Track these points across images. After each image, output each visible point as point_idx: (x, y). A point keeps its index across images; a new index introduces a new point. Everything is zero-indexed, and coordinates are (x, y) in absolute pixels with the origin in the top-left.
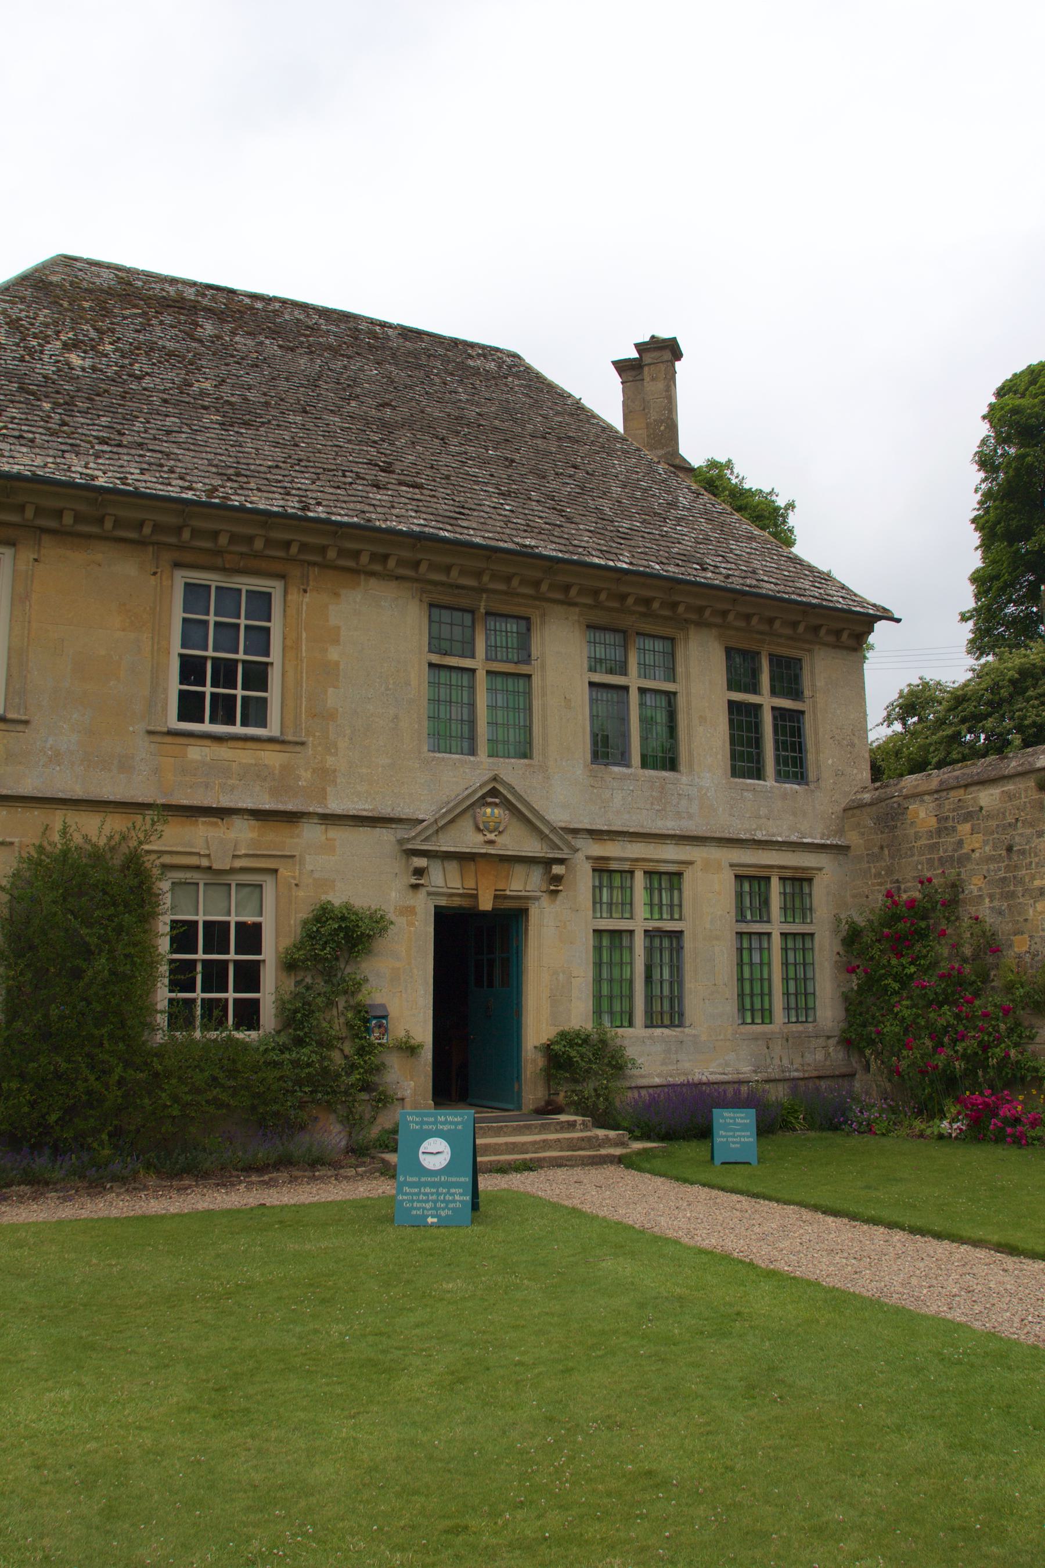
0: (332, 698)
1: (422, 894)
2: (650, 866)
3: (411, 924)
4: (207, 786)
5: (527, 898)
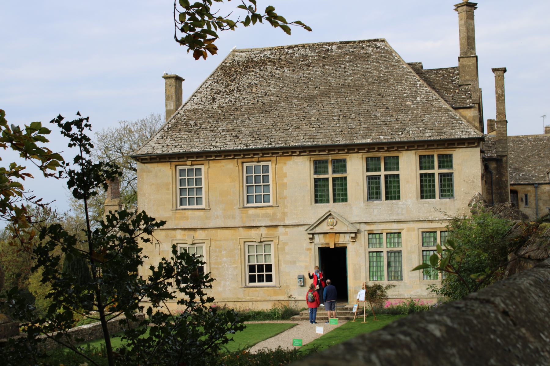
0: (286, 193)
1: (313, 244)
2: (388, 231)
3: (310, 253)
4: (254, 220)
5: (345, 244)
